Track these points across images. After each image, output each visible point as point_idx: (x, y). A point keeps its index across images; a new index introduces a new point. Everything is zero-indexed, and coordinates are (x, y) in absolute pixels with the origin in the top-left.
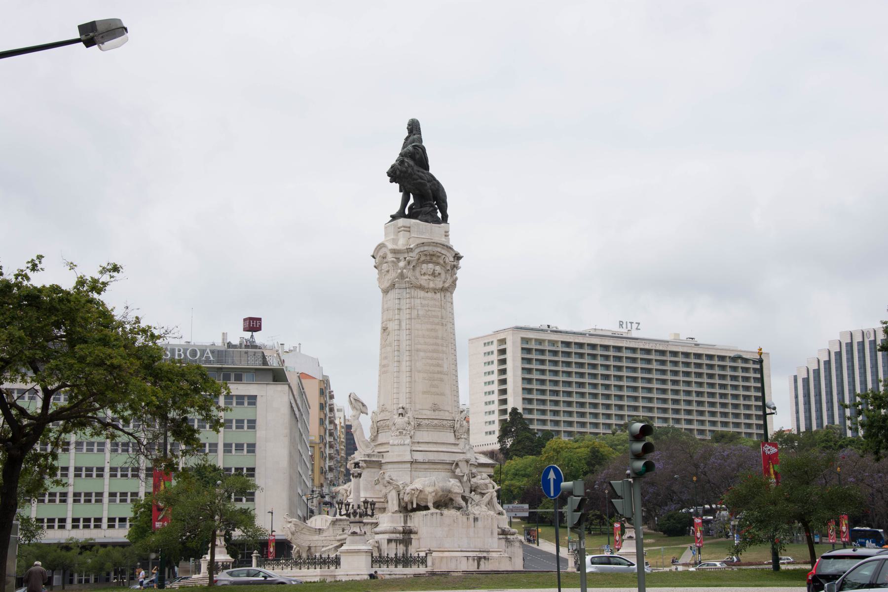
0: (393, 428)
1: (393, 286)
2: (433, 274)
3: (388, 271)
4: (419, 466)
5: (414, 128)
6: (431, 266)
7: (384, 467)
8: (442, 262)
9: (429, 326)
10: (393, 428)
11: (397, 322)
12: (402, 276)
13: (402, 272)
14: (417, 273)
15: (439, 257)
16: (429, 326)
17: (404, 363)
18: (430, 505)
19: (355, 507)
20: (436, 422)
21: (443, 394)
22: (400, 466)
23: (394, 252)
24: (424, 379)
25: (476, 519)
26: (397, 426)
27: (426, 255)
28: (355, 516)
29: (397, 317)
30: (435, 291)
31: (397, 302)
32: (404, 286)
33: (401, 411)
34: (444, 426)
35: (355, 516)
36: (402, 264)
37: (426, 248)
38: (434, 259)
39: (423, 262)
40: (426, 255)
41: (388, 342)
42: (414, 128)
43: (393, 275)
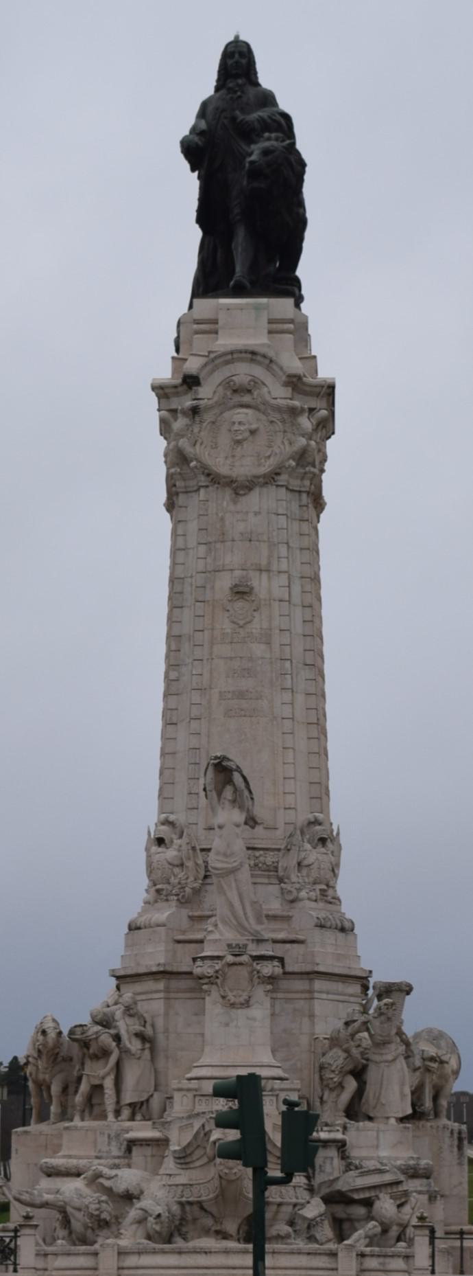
1: (271, 478)
3: (253, 432)
5: (237, 64)
7: (284, 984)
11: (284, 577)
12: (302, 457)
13: (308, 445)
17: (300, 699)
22: (340, 986)
23: (295, 383)
26: (314, 874)
29: (284, 566)
31: (283, 519)
32: (295, 484)
36: (306, 423)
41: (256, 627)
42: (237, 64)
43: (283, 448)
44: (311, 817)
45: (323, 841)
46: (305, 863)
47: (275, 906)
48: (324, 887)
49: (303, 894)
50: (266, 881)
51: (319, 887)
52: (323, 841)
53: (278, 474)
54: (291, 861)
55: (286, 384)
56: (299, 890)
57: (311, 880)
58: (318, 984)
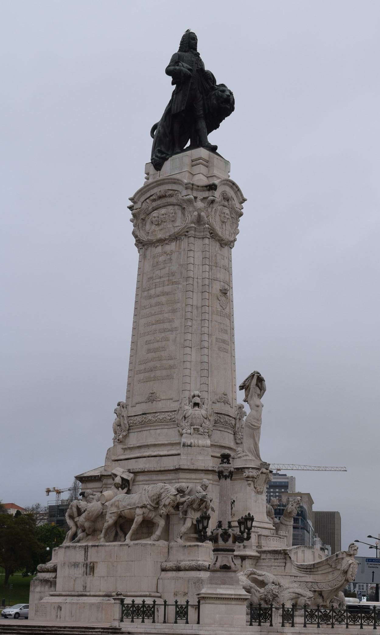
0: (183, 423)
10: (183, 423)
12: (199, 220)
19: (225, 526)
28: (225, 540)
33: (197, 400)
35: (225, 540)
44: (192, 394)
45: (196, 405)
46: (186, 416)
47: (176, 439)
48: (197, 427)
49: (184, 431)
50: (172, 426)
51: (192, 427)
52: (196, 405)
53: (187, 232)
54: (179, 417)
55: (187, 188)
56: (183, 430)
57: (189, 424)
58: (182, 475)
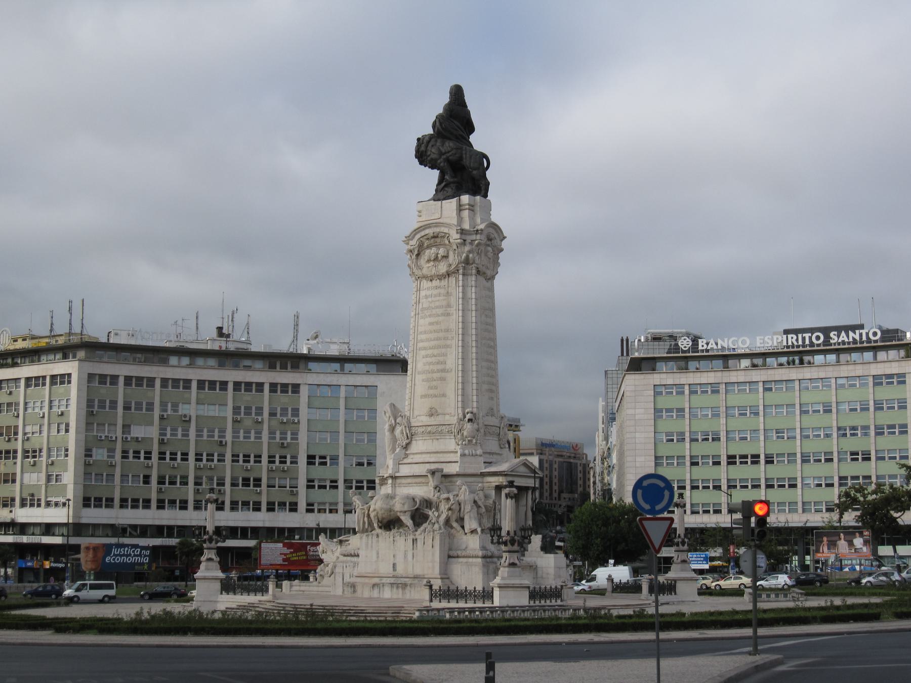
2: (436, 259)
4: (404, 481)
5: (457, 94)
6: (434, 250)
8: (447, 242)
9: (432, 320)
14: (422, 261)
15: (444, 237)
16: (432, 320)
18: (375, 525)
20: (429, 429)
21: (444, 395)
24: (423, 380)
25: (414, 541)
27: (428, 239)
30: (441, 277)
34: (441, 433)
37: (427, 231)
38: (438, 240)
39: (429, 247)
40: (428, 239)
42: (457, 94)
